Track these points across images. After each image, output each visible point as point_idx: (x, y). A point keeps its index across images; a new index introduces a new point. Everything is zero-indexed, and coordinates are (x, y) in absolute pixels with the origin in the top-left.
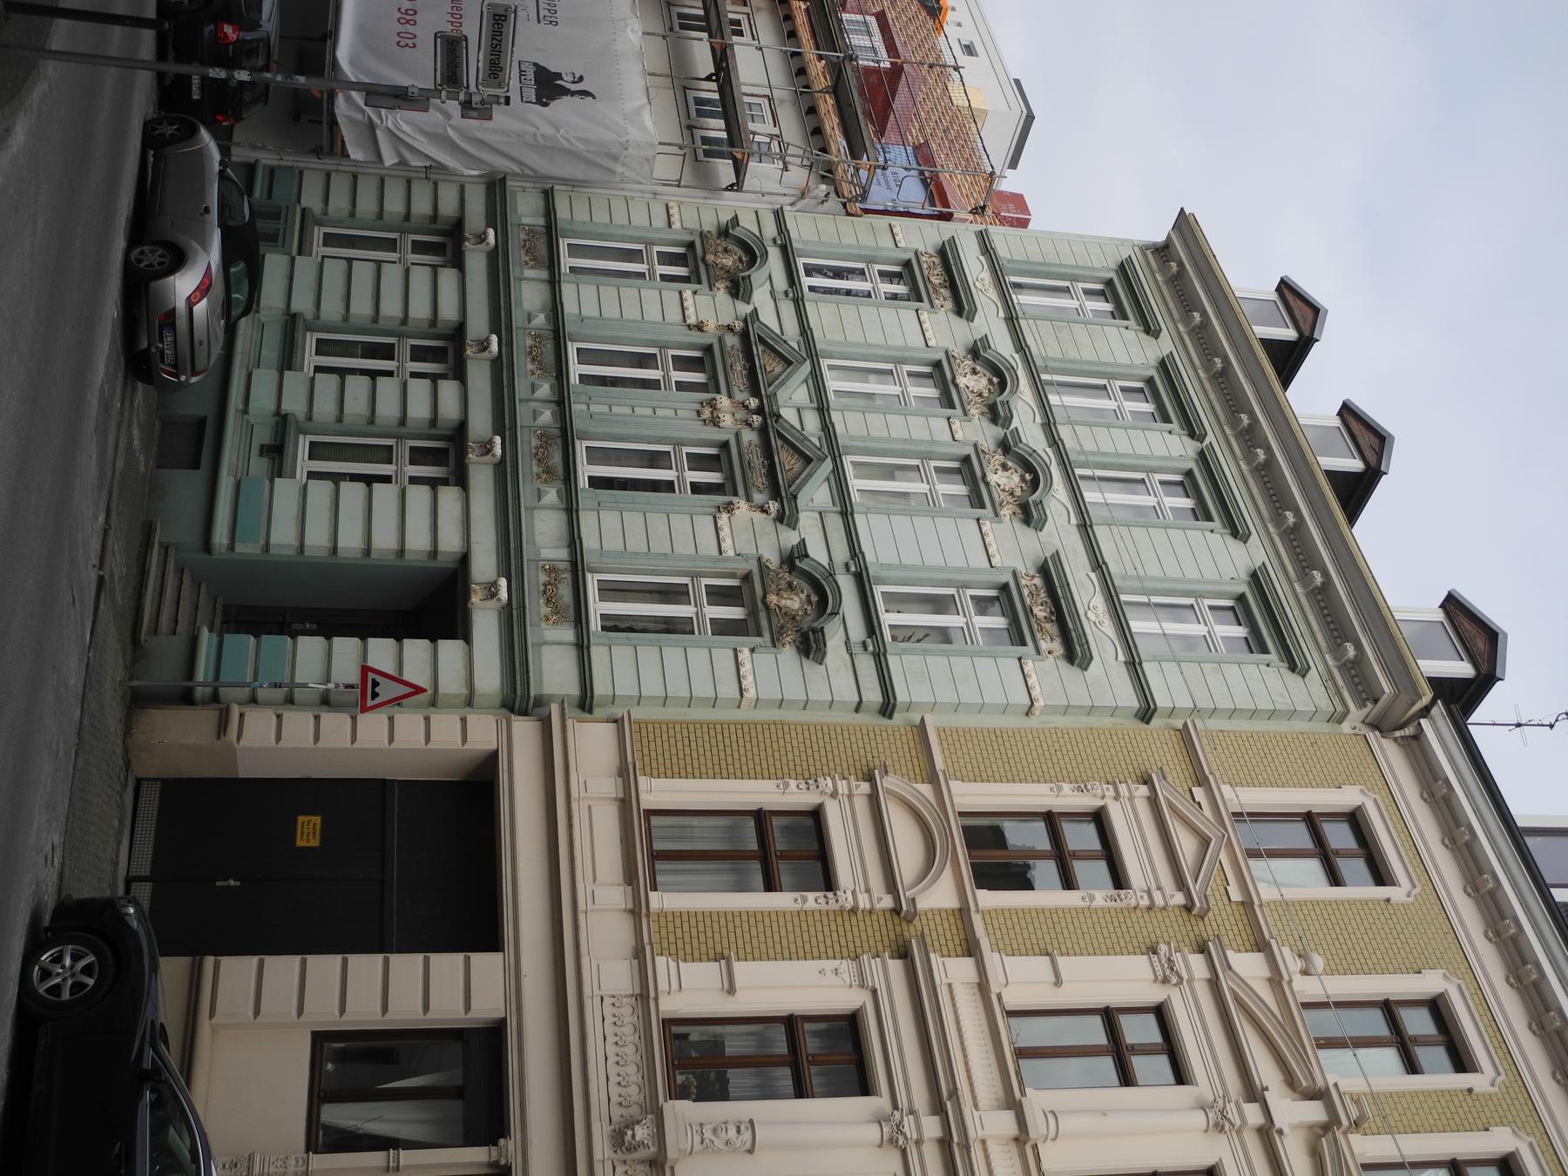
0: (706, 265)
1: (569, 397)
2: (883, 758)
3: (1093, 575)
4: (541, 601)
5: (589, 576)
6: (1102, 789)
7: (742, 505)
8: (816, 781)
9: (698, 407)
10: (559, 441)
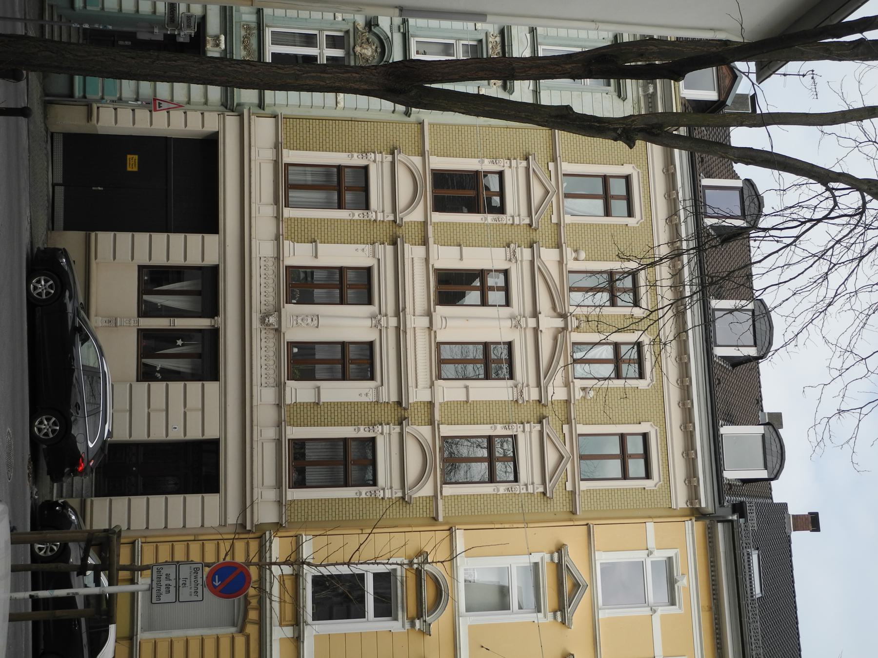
3: (528, 35)
4: (242, 47)
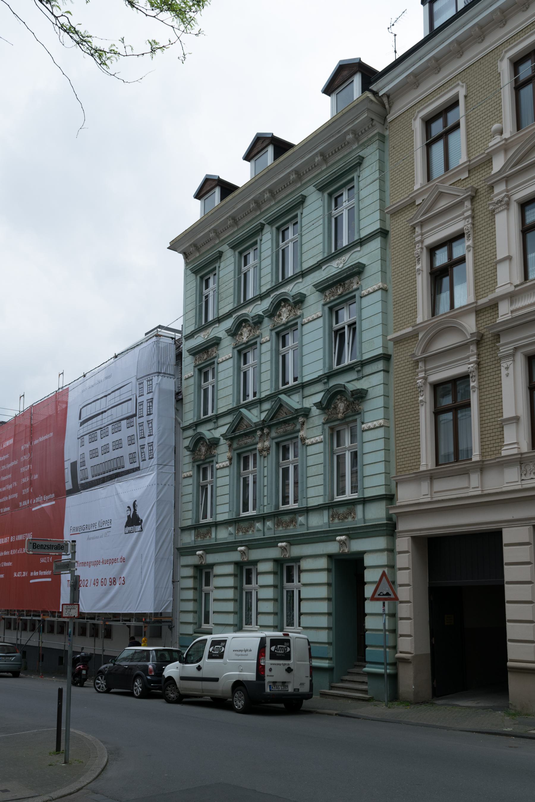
0: (206, 459)
1: (261, 514)
3: (323, 268)
4: (346, 521)
5: (335, 500)
6: (418, 249)
7: (302, 433)
8: (419, 387)
10: (279, 517)
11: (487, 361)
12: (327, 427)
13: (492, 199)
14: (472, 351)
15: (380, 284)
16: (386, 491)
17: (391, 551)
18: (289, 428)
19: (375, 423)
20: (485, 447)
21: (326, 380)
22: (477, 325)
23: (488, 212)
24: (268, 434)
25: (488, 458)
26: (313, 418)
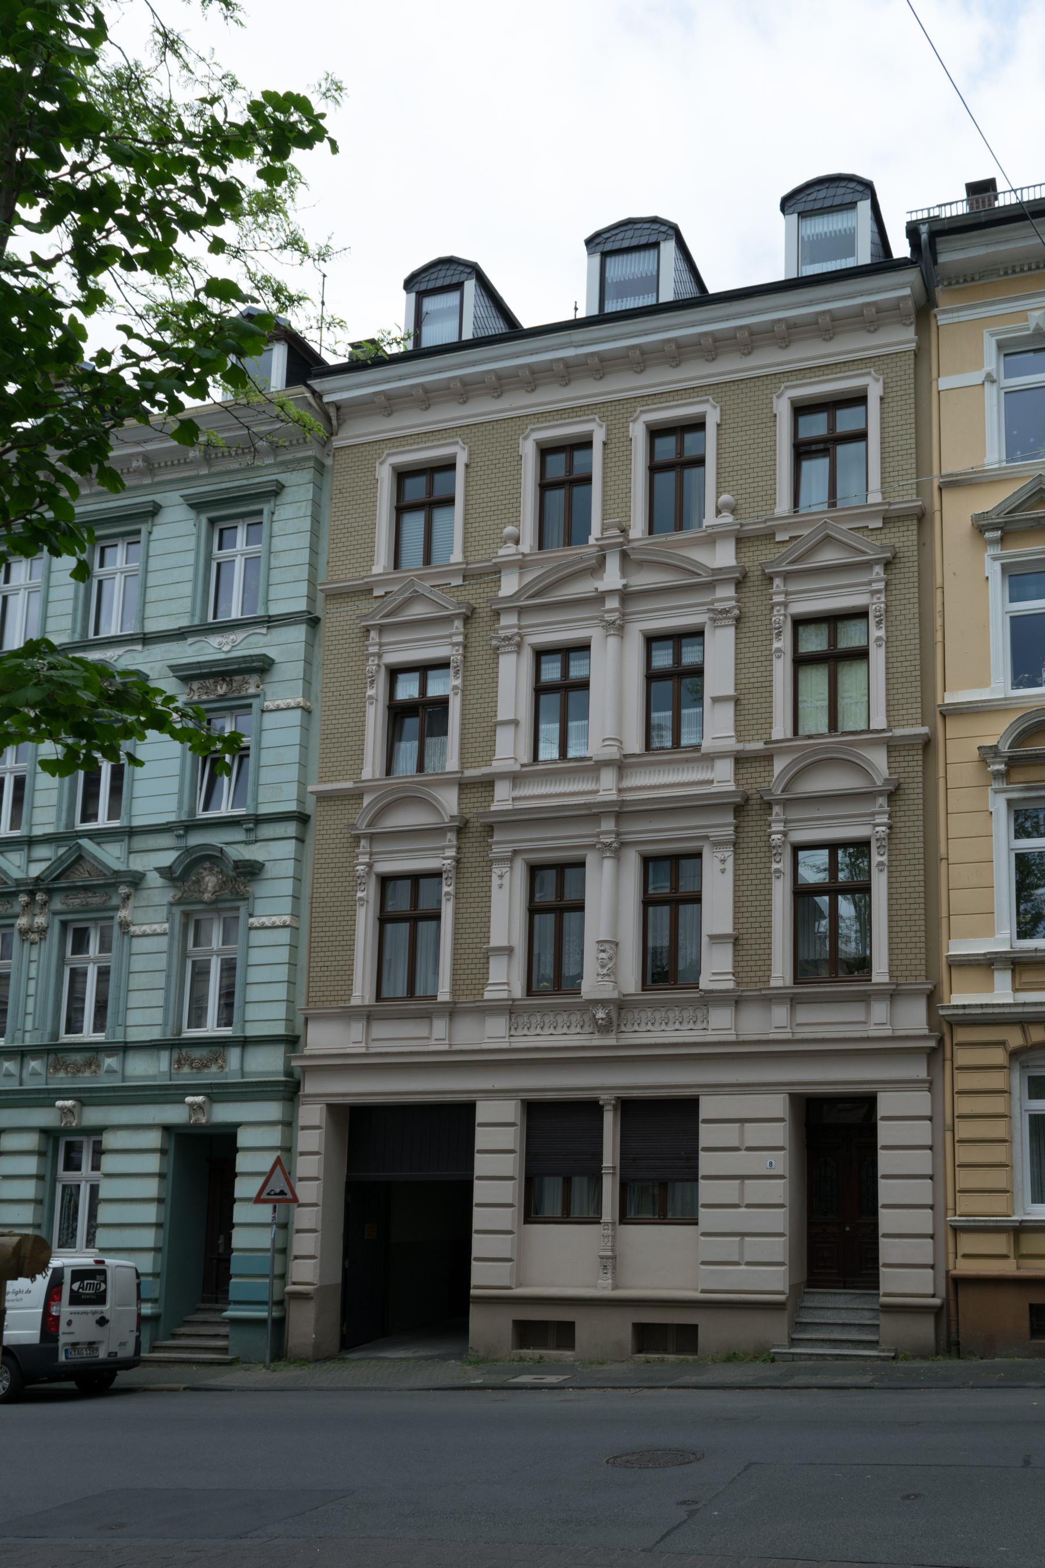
2: (342, 826)
3: (190, 640)
5: (184, 1035)
7: (123, 914)
9: (26, 945)
10: (60, 1055)
11: (471, 860)
12: (177, 911)
13: (496, 630)
14: (450, 841)
15: (300, 700)
16: (286, 1029)
17: (288, 1124)
18: (96, 900)
19: (274, 919)
20: (459, 982)
21: (182, 832)
22: (459, 804)
23: (488, 647)
24: (45, 904)
25: (463, 999)
26: (149, 891)
